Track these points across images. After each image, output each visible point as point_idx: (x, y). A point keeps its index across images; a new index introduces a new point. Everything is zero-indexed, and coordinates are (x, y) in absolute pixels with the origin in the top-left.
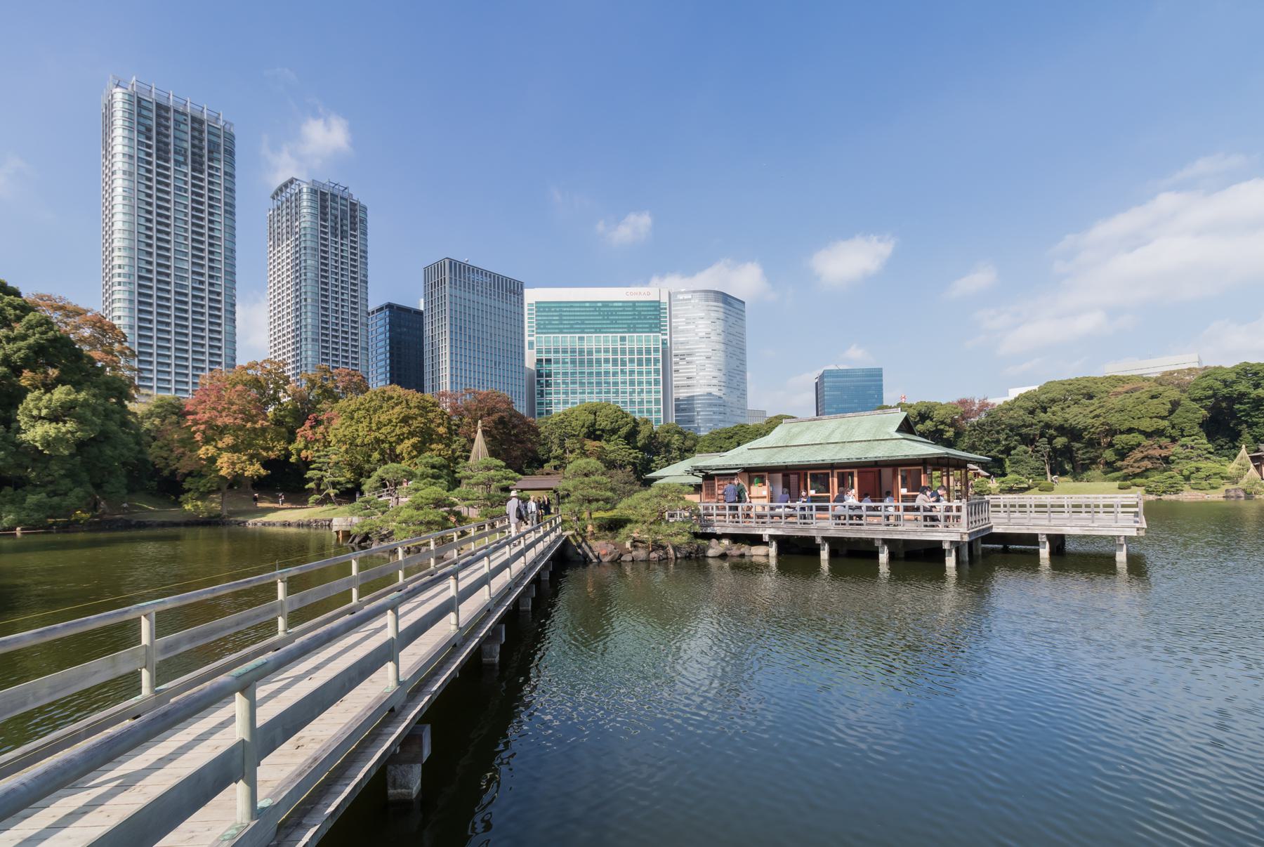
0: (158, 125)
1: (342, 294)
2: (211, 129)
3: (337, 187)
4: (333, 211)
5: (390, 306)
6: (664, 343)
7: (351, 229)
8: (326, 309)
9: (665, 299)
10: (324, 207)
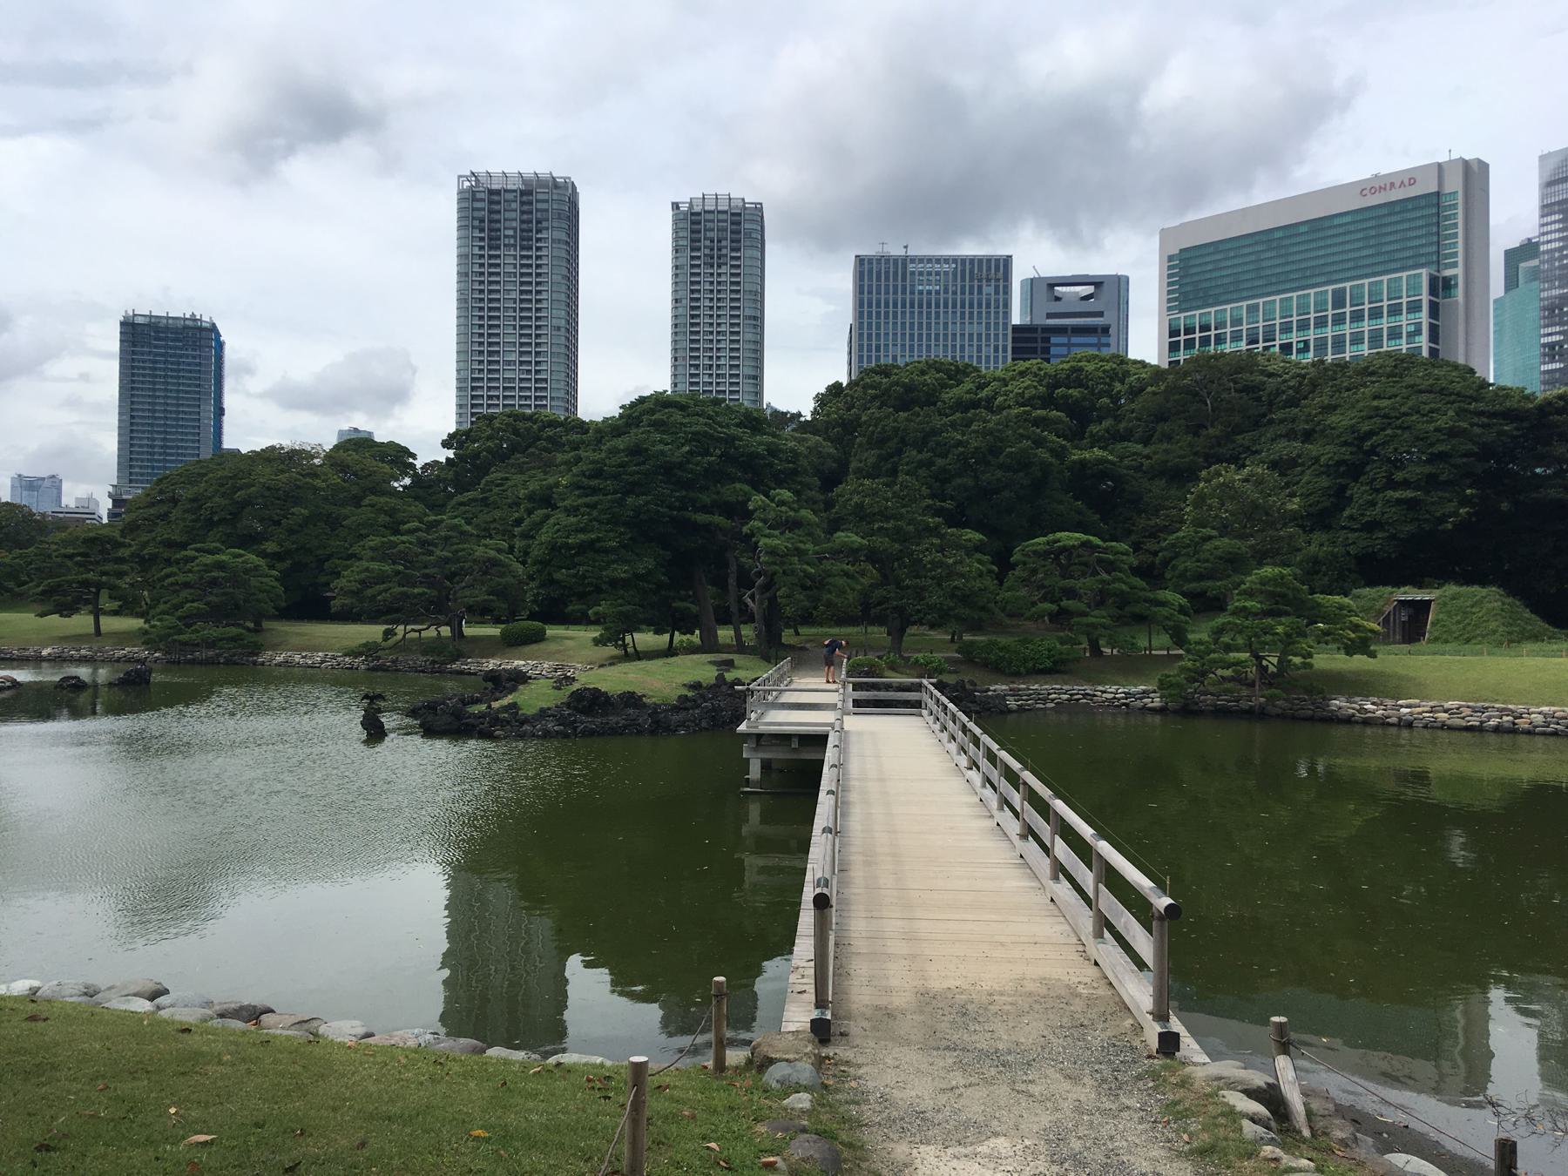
8: (697, 367)
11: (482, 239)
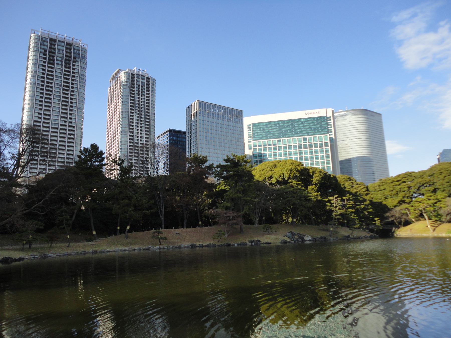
0: (50, 48)
1: (141, 124)
2: (76, 48)
3: (140, 71)
4: (138, 83)
5: (170, 131)
6: (331, 139)
7: (147, 91)
9: (330, 114)
10: (133, 81)
11: (45, 58)
